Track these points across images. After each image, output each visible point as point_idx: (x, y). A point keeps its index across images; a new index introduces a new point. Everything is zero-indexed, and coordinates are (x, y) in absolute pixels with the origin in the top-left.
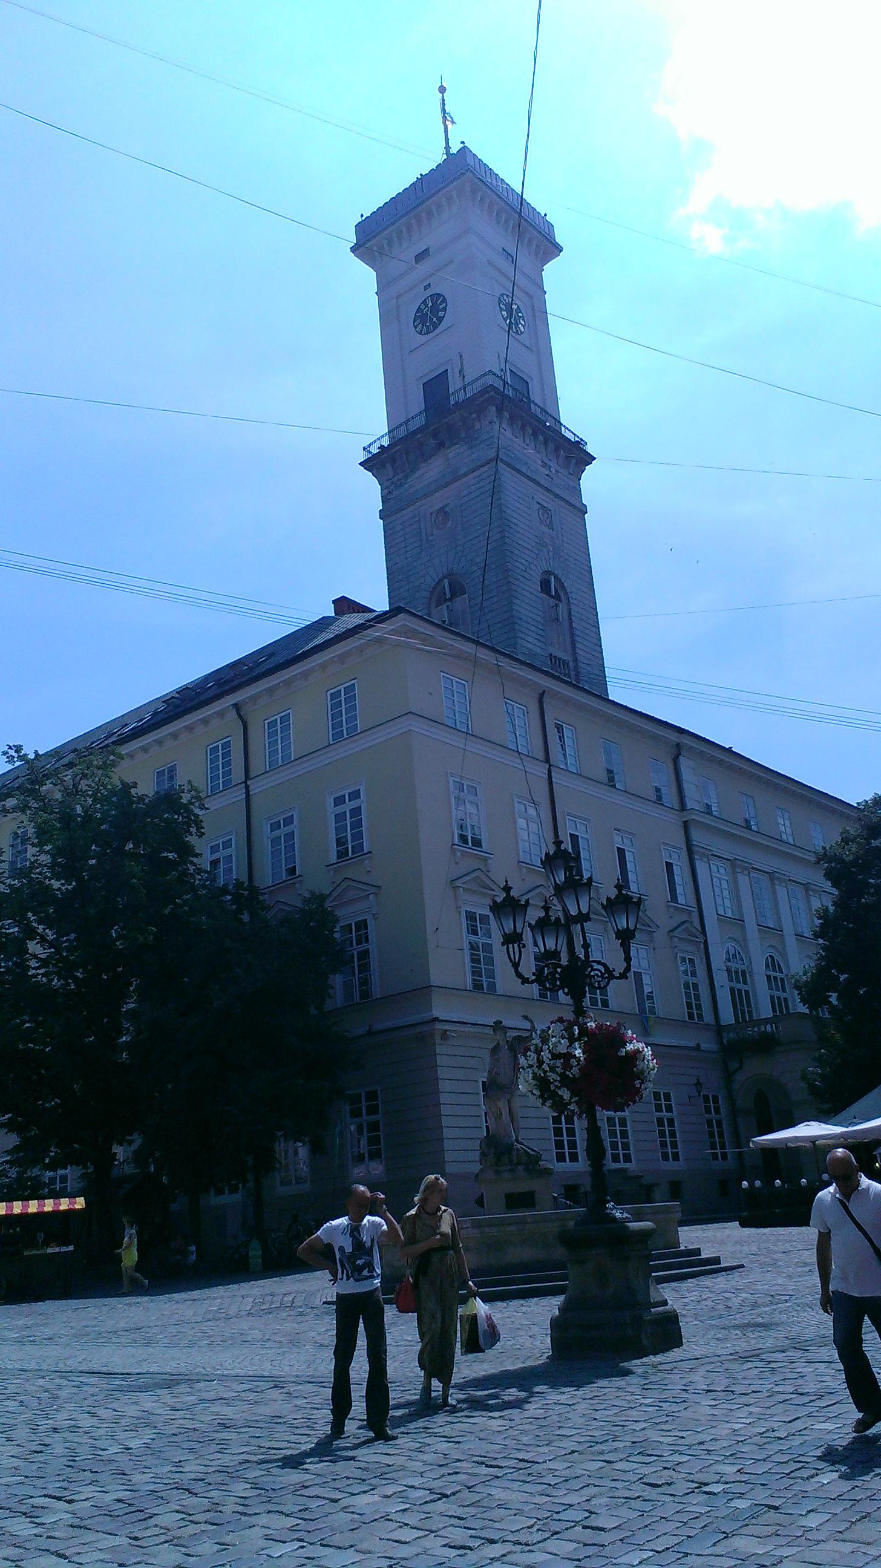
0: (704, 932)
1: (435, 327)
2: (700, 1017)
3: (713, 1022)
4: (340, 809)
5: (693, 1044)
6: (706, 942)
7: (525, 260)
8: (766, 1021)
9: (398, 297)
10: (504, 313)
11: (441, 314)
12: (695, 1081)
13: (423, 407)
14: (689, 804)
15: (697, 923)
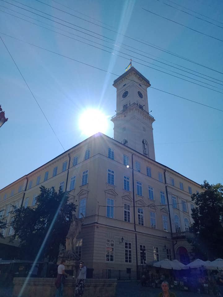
0: (169, 211)
4: (84, 174)
6: (169, 213)
8: (184, 232)
12: (164, 245)
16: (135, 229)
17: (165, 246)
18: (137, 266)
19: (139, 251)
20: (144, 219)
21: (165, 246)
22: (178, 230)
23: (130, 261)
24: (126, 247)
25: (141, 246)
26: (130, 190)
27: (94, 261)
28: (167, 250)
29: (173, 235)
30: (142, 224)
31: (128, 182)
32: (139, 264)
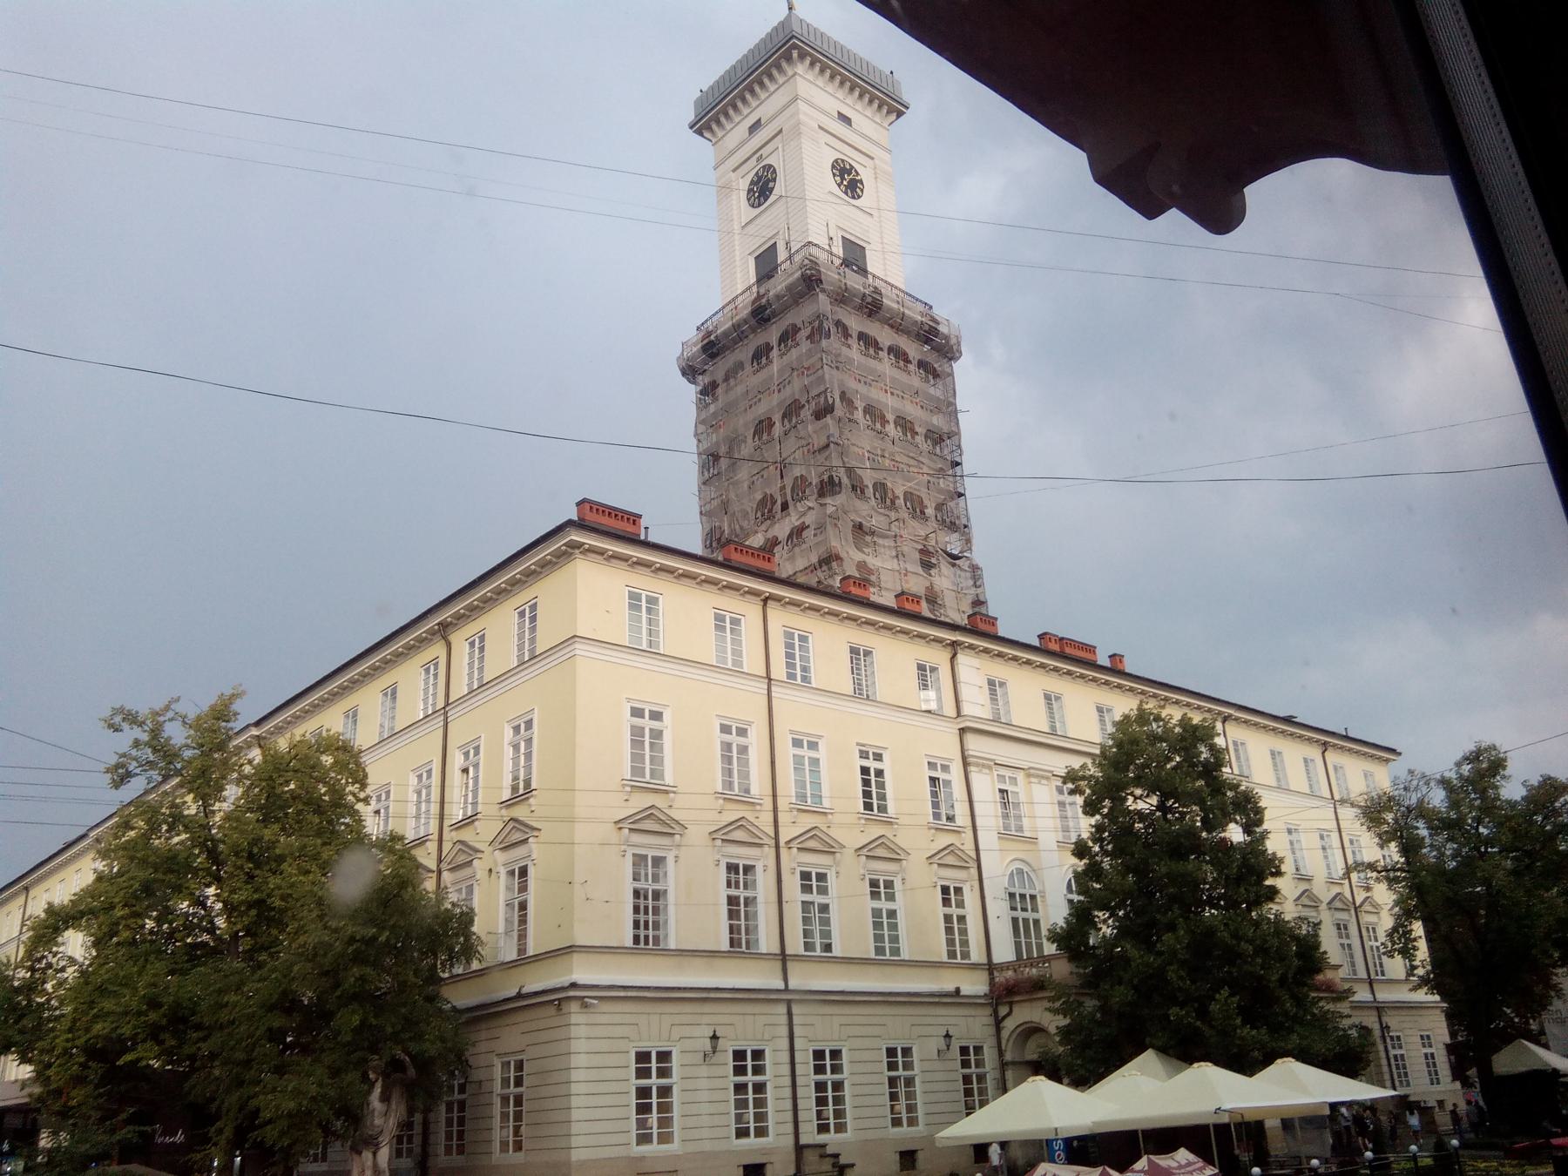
1: (766, 200)
2: (966, 955)
3: (984, 960)
5: (949, 987)
7: (866, 120)
9: (734, 171)
10: (838, 179)
11: (771, 185)
13: (753, 279)
14: (967, 709)
15: (969, 847)
16: (786, 980)
17: (948, 1036)
18: (800, 1149)
19: (807, 1076)
20: (834, 915)
21: (948, 1036)
22: (1029, 945)
23: (761, 1132)
24: (740, 1070)
25: (819, 1055)
26: (754, 790)
27: (576, 1156)
28: (964, 1050)
29: (996, 974)
30: (828, 948)
31: (743, 750)
32: (810, 1135)
